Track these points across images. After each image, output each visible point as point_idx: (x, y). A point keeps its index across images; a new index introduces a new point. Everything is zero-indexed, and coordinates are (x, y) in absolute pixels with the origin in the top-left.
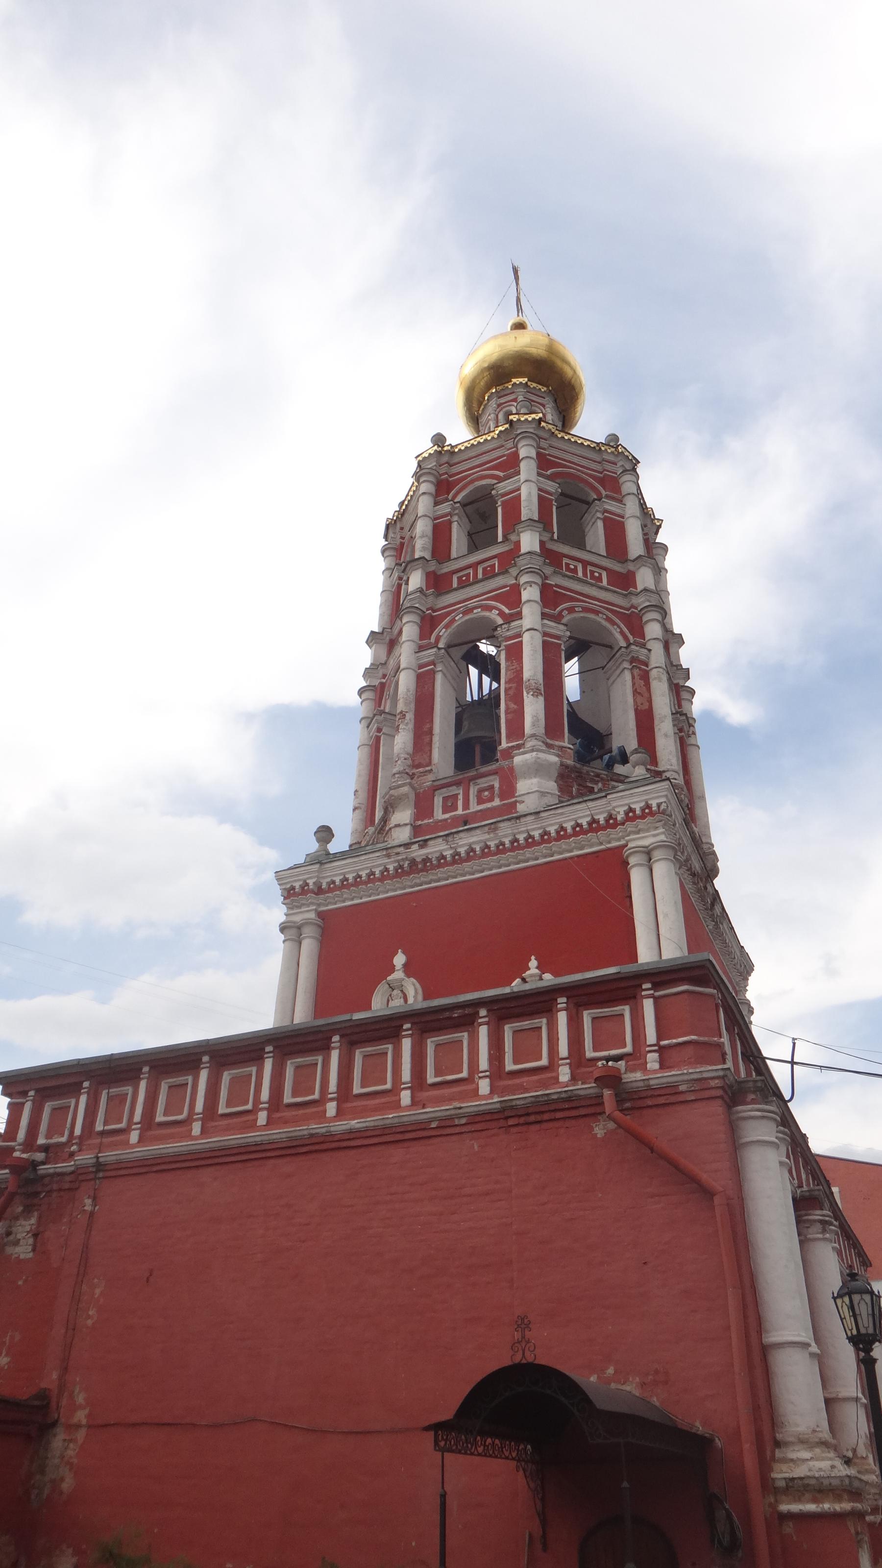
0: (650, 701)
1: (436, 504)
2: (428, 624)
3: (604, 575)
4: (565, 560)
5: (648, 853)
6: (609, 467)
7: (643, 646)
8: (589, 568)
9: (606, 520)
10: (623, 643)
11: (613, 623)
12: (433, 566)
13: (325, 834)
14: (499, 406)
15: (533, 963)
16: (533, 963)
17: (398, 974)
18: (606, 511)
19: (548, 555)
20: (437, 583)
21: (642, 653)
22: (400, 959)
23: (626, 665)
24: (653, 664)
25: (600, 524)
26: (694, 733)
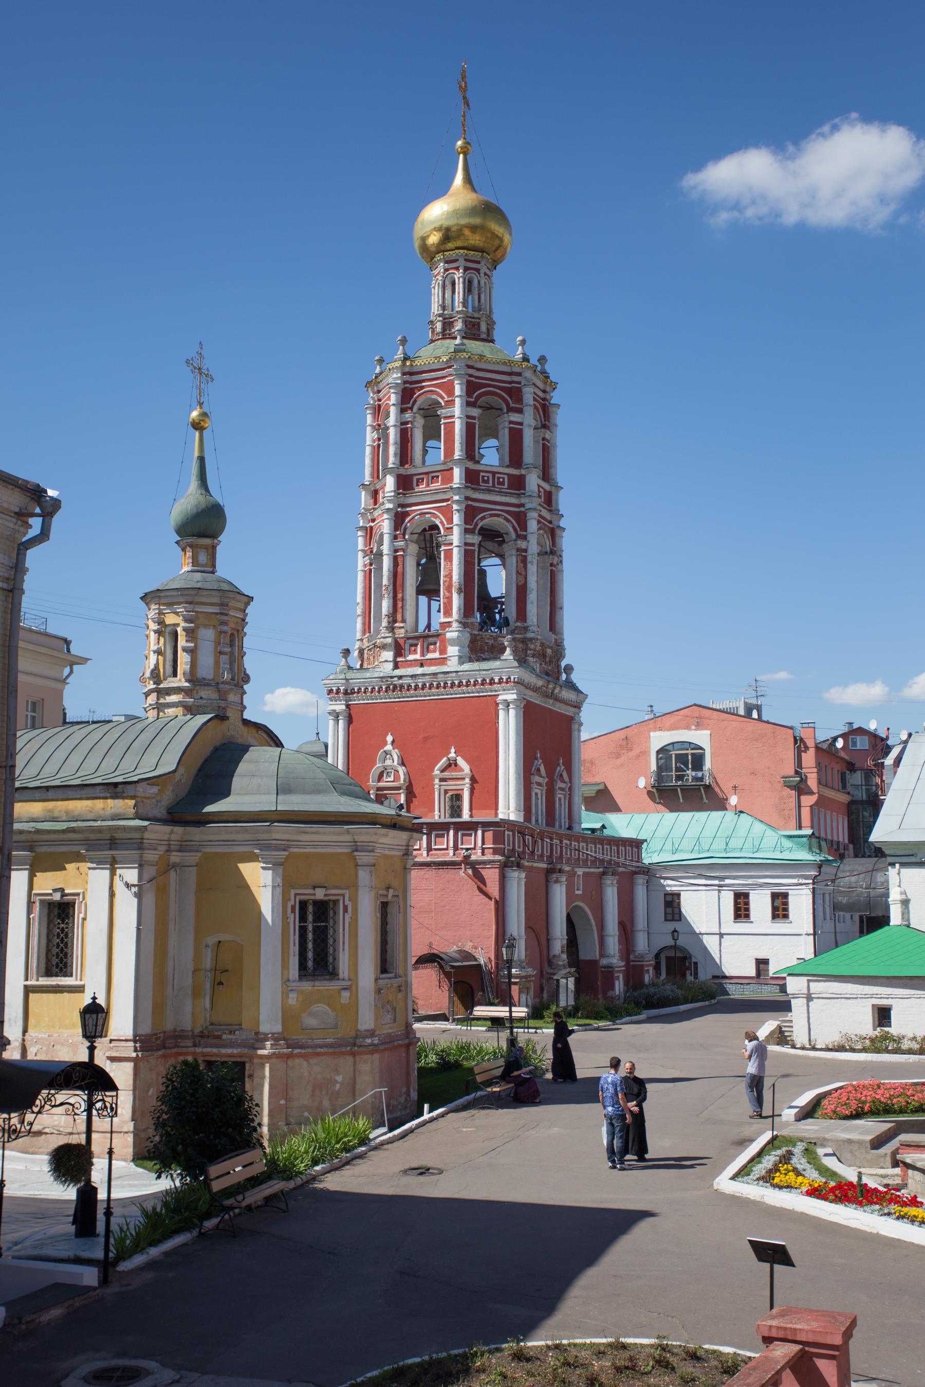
0: (526, 578)
1: (403, 411)
2: (399, 519)
3: (506, 477)
4: (482, 474)
5: (507, 704)
6: (515, 378)
7: (525, 538)
8: (497, 475)
9: (510, 429)
10: (514, 536)
11: (508, 521)
12: (402, 471)
13: (347, 652)
14: (446, 270)
15: (453, 750)
16: (453, 750)
17: (389, 747)
18: (511, 422)
19: (472, 477)
20: (405, 483)
21: (522, 544)
22: (389, 738)
23: (514, 552)
24: (529, 552)
25: (507, 431)
26: (561, 562)
